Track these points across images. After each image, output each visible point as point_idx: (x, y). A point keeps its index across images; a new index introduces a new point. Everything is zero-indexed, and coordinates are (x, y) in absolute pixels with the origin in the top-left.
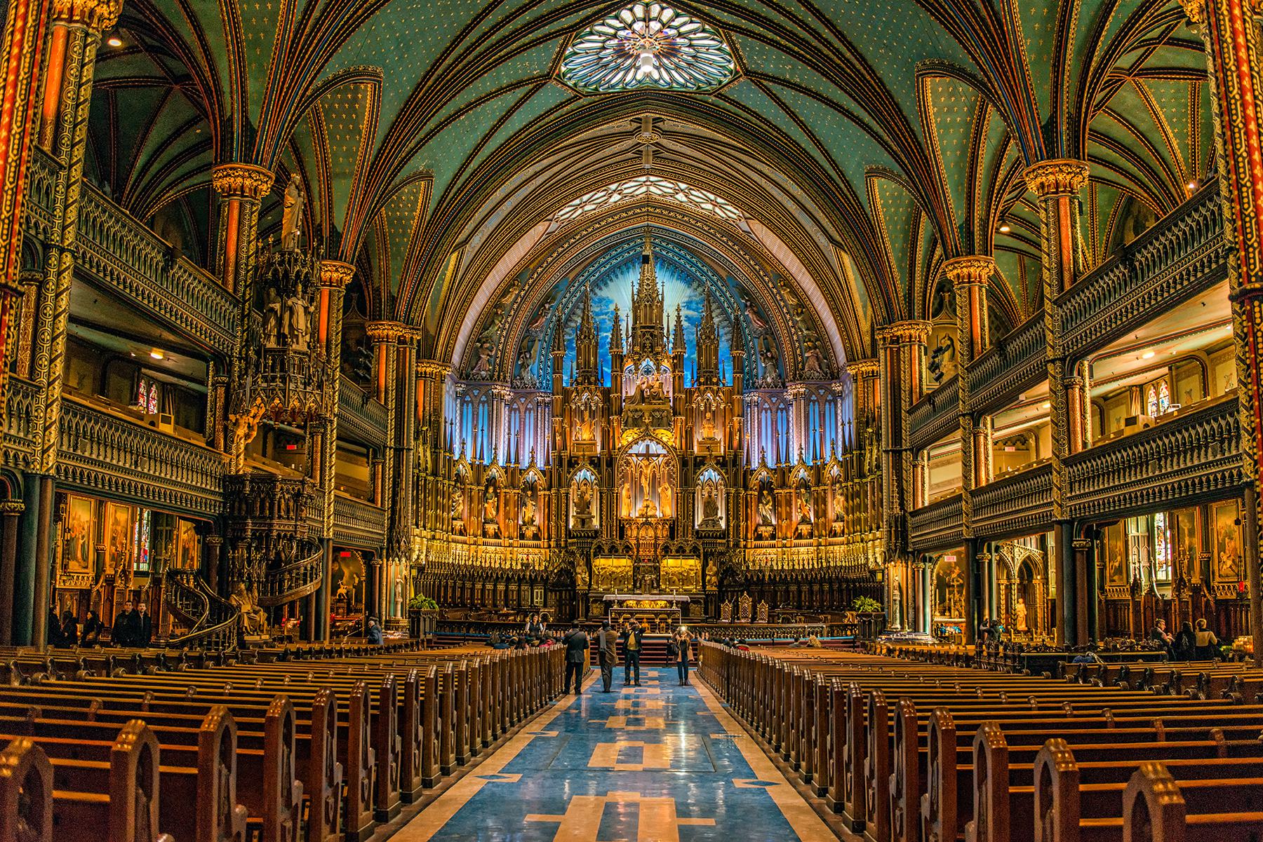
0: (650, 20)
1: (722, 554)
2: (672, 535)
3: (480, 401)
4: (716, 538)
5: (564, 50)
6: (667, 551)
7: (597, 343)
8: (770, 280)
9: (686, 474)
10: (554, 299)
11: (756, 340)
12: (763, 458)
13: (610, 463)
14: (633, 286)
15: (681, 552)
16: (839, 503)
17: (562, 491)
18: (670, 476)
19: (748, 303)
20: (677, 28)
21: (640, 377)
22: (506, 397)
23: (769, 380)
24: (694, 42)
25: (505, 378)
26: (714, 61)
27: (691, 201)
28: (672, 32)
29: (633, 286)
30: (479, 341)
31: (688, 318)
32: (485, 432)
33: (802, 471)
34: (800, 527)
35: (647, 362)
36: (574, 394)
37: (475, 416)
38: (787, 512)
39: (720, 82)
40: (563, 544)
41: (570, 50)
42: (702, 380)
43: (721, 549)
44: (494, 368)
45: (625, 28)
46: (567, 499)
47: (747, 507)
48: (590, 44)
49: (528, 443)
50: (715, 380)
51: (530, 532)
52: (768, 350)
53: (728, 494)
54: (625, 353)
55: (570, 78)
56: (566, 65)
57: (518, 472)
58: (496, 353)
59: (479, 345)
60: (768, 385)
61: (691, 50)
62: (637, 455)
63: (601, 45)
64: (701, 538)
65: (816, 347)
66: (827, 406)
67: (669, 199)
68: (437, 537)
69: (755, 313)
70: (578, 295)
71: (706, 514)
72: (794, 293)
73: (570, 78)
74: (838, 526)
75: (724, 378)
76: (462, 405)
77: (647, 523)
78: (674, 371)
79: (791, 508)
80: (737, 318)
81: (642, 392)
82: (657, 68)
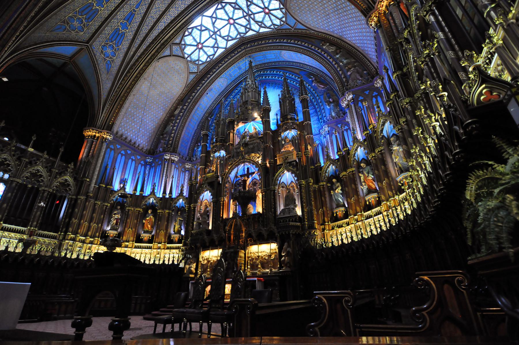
8: (316, 47)
11: (322, 97)
17: (192, 205)
19: (313, 79)
23: (333, 114)
27: (261, 24)
30: (162, 135)
34: (367, 198)
37: (155, 173)
38: (352, 189)
44: (167, 146)
46: (194, 212)
51: (176, 237)
53: (300, 185)
59: (162, 137)
65: (355, 67)
67: (251, 33)
69: (318, 82)
71: (286, 205)
72: (332, 44)
76: (150, 169)
79: (356, 185)
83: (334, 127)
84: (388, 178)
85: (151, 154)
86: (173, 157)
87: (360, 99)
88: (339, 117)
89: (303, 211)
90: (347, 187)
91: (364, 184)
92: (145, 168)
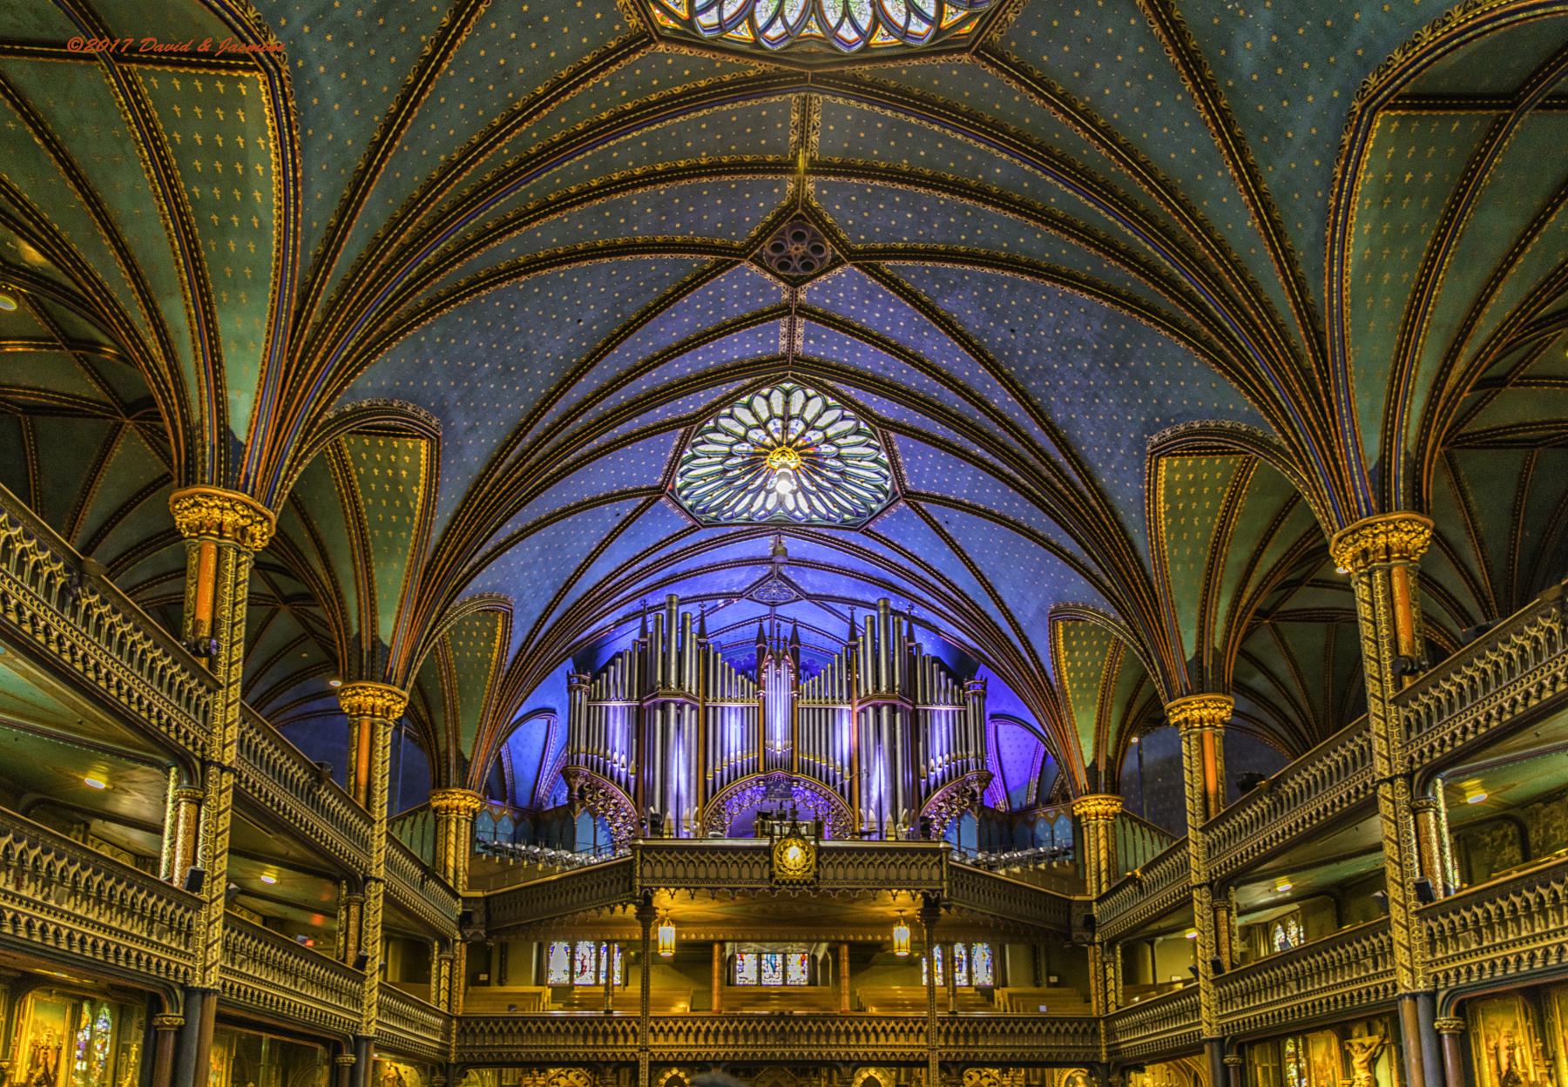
0: (791, 418)
5: (683, 451)
20: (822, 429)
24: (843, 451)
26: (867, 480)
28: (815, 436)
39: (872, 510)
41: (688, 452)
45: (758, 427)
48: (717, 444)
55: (686, 498)
56: (682, 475)
61: (839, 464)
63: (727, 449)
73: (686, 498)
82: (794, 493)
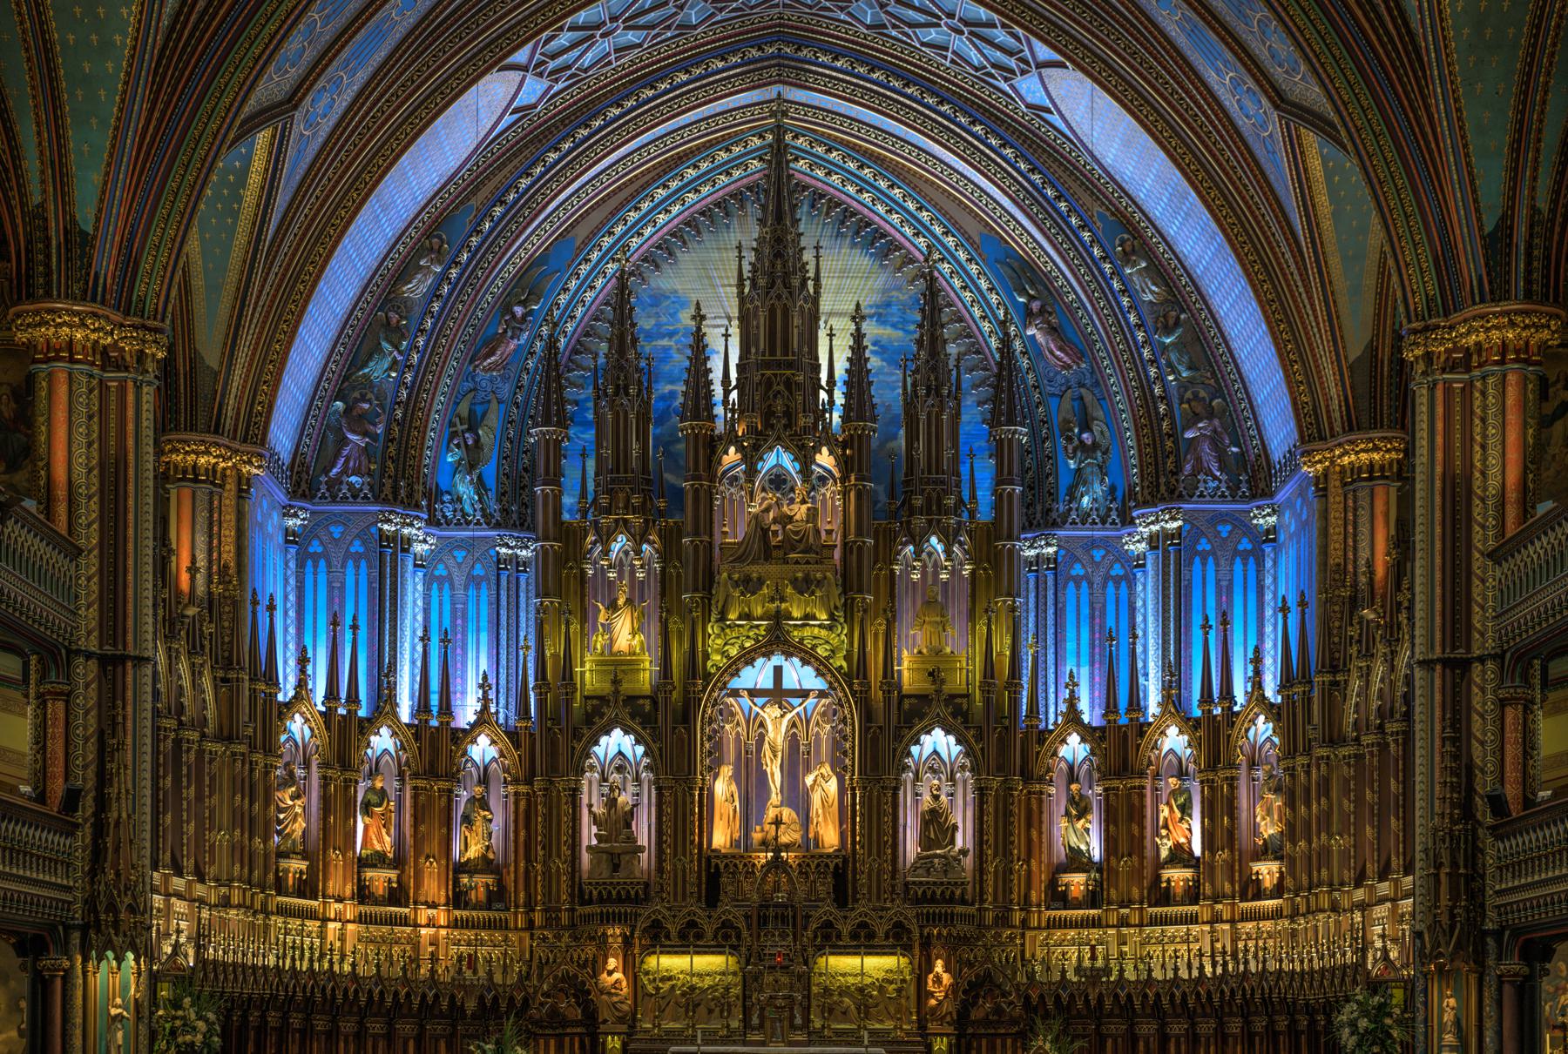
1: (965, 940)
2: (842, 895)
3: (348, 555)
4: (951, 900)
6: (831, 941)
7: (647, 404)
9: (875, 740)
10: (534, 294)
11: (1054, 402)
12: (1072, 702)
13: (686, 715)
14: (741, 258)
15: (864, 942)
16: (1269, 812)
18: (836, 745)
19: (1035, 306)
21: (759, 496)
22: (419, 548)
25: (410, 495)
29: (741, 258)
31: (882, 348)
32: (363, 634)
33: (1173, 731)
34: (1167, 873)
35: (778, 458)
36: (591, 538)
40: (565, 918)
42: (918, 501)
43: (962, 928)
44: (383, 468)
47: (1029, 826)
49: (476, 663)
50: (950, 501)
52: (1086, 426)
53: (981, 791)
54: (720, 427)
57: (446, 737)
58: (388, 430)
60: (1085, 518)
62: (753, 693)
64: (918, 901)
66: (1238, 566)
68: (235, 900)
69: (1053, 330)
70: (599, 283)
71: (926, 842)
74: (1267, 871)
75: (973, 496)
76: (301, 565)
77: (777, 864)
78: (844, 479)
80: (1006, 342)
81: (765, 531)
83: (1079, 553)
84: (1232, 850)
85: (304, 496)
86: (411, 525)
87: (1200, 548)
88: (1104, 522)
89: (980, 869)
90: (1116, 825)
91: (1164, 832)
92: (286, 564)
